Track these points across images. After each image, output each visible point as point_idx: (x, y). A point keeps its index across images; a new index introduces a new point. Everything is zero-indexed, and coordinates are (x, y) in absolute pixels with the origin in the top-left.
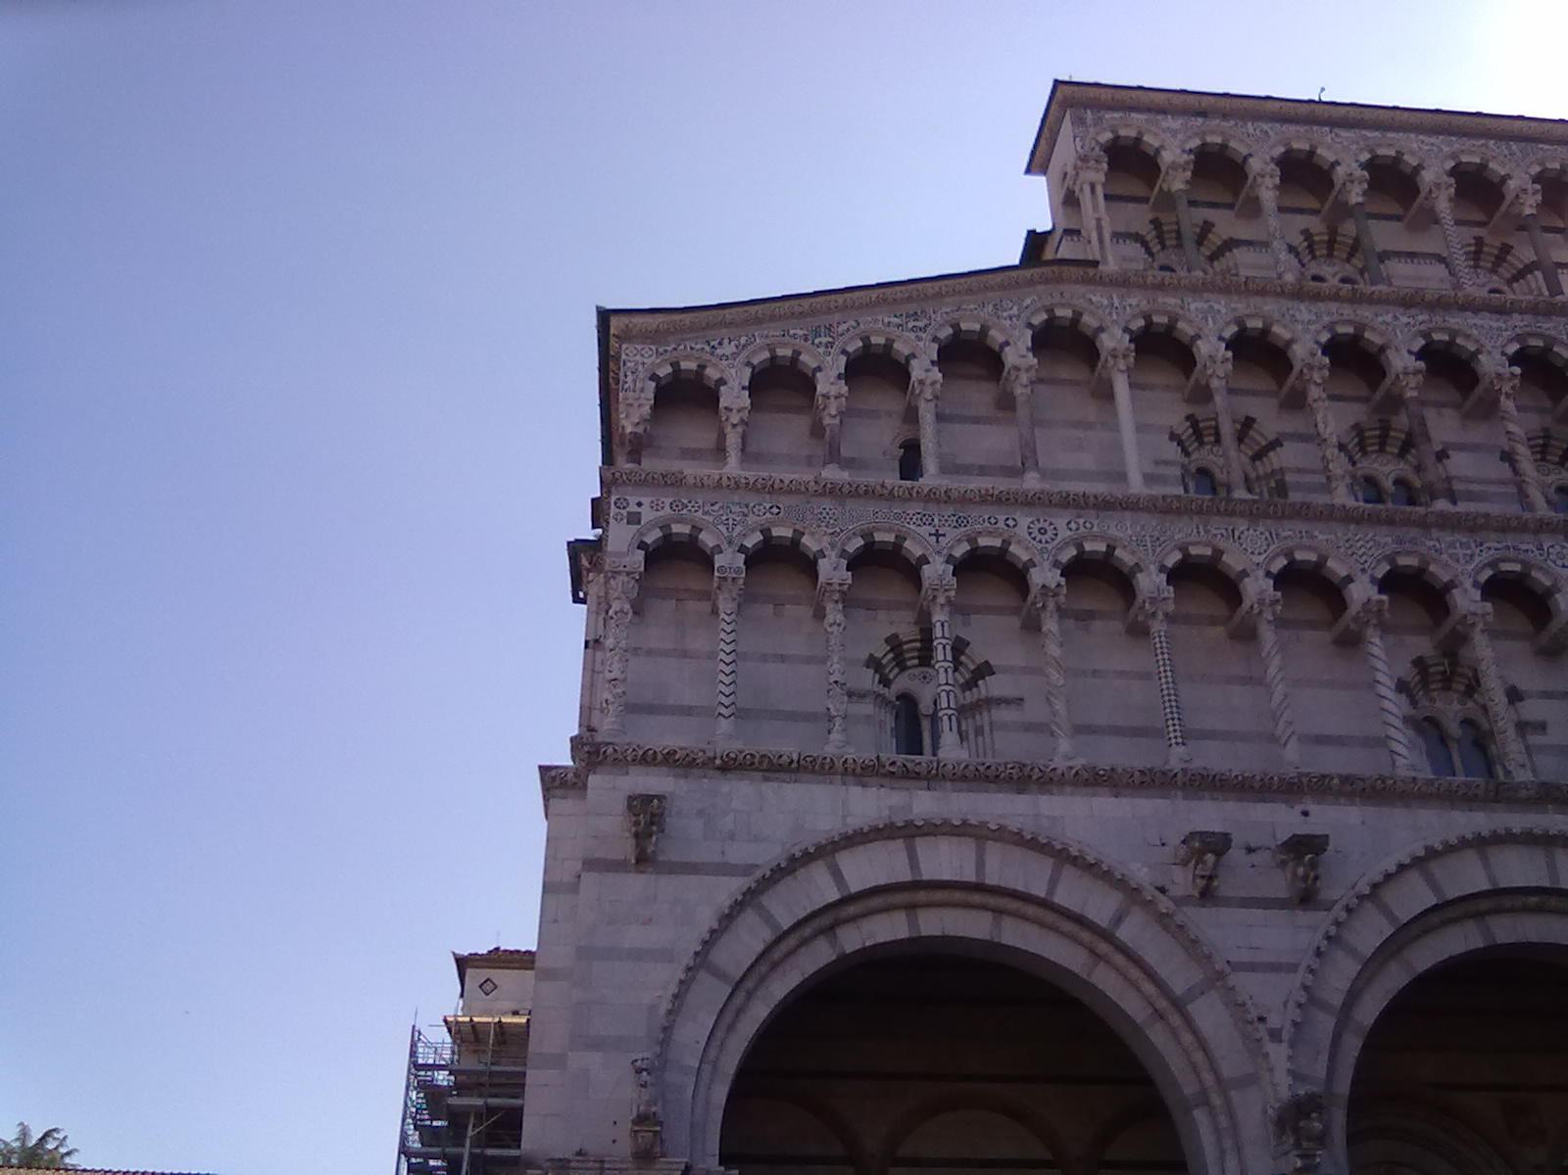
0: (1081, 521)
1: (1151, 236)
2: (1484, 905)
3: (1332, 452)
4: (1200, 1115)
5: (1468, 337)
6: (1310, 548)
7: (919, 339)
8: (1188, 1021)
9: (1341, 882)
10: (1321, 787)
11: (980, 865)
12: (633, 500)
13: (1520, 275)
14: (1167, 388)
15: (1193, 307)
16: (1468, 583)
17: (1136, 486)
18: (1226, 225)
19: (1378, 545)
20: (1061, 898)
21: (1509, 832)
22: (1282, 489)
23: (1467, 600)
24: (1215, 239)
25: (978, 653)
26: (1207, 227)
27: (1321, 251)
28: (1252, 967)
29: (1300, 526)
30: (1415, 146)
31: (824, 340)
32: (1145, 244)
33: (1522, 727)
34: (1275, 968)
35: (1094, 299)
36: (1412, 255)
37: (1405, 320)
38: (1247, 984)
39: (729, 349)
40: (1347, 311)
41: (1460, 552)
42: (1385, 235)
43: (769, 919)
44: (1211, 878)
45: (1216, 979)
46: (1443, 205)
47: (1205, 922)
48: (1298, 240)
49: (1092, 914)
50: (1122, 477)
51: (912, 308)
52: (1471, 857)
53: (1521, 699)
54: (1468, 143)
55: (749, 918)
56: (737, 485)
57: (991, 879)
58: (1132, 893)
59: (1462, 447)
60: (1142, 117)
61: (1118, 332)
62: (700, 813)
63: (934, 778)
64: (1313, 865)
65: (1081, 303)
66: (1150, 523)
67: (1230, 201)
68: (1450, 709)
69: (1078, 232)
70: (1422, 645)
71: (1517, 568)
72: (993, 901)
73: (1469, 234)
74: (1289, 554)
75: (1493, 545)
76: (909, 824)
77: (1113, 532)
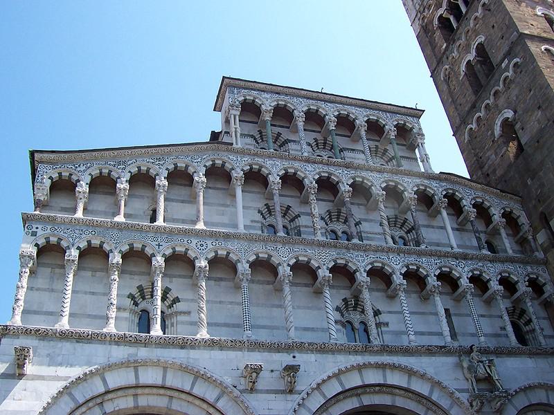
0: (217, 242)
2: (359, 391)
3: (317, 220)
5: (368, 180)
6: (305, 256)
7: (160, 168)
9: (303, 384)
10: (300, 347)
11: (164, 377)
12: (35, 226)
13: (391, 160)
14: (259, 193)
15: (268, 163)
16: (362, 270)
17: (241, 230)
18: (286, 134)
20: (196, 391)
21: (370, 363)
22: (299, 234)
23: (362, 277)
24: (282, 139)
30: (354, 111)
31: (122, 167)
32: (255, 139)
33: (378, 325)
36: (353, 150)
39: (82, 168)
40: (326, 168)
42: (341, 142)
43: (74, 399)
44: (254, 383)
46: (363, 133)
48: (312, 142)
50: (236, 226)
53: (381, 314)
54: (372, 112)
55: (66, 398)
57: (168, 384)
58: (224, 390)
59: (365, 220)
61: (239, 170)
62: (48, 355)
63: (147, 343)
68: (356, 318)
69: (228, 133)
70: (346, 294)
71: (380, 265)
72: (169, 393)
73: (373, 144)
74: (297, 258)
75: (372, 257)
76: (136, 361)
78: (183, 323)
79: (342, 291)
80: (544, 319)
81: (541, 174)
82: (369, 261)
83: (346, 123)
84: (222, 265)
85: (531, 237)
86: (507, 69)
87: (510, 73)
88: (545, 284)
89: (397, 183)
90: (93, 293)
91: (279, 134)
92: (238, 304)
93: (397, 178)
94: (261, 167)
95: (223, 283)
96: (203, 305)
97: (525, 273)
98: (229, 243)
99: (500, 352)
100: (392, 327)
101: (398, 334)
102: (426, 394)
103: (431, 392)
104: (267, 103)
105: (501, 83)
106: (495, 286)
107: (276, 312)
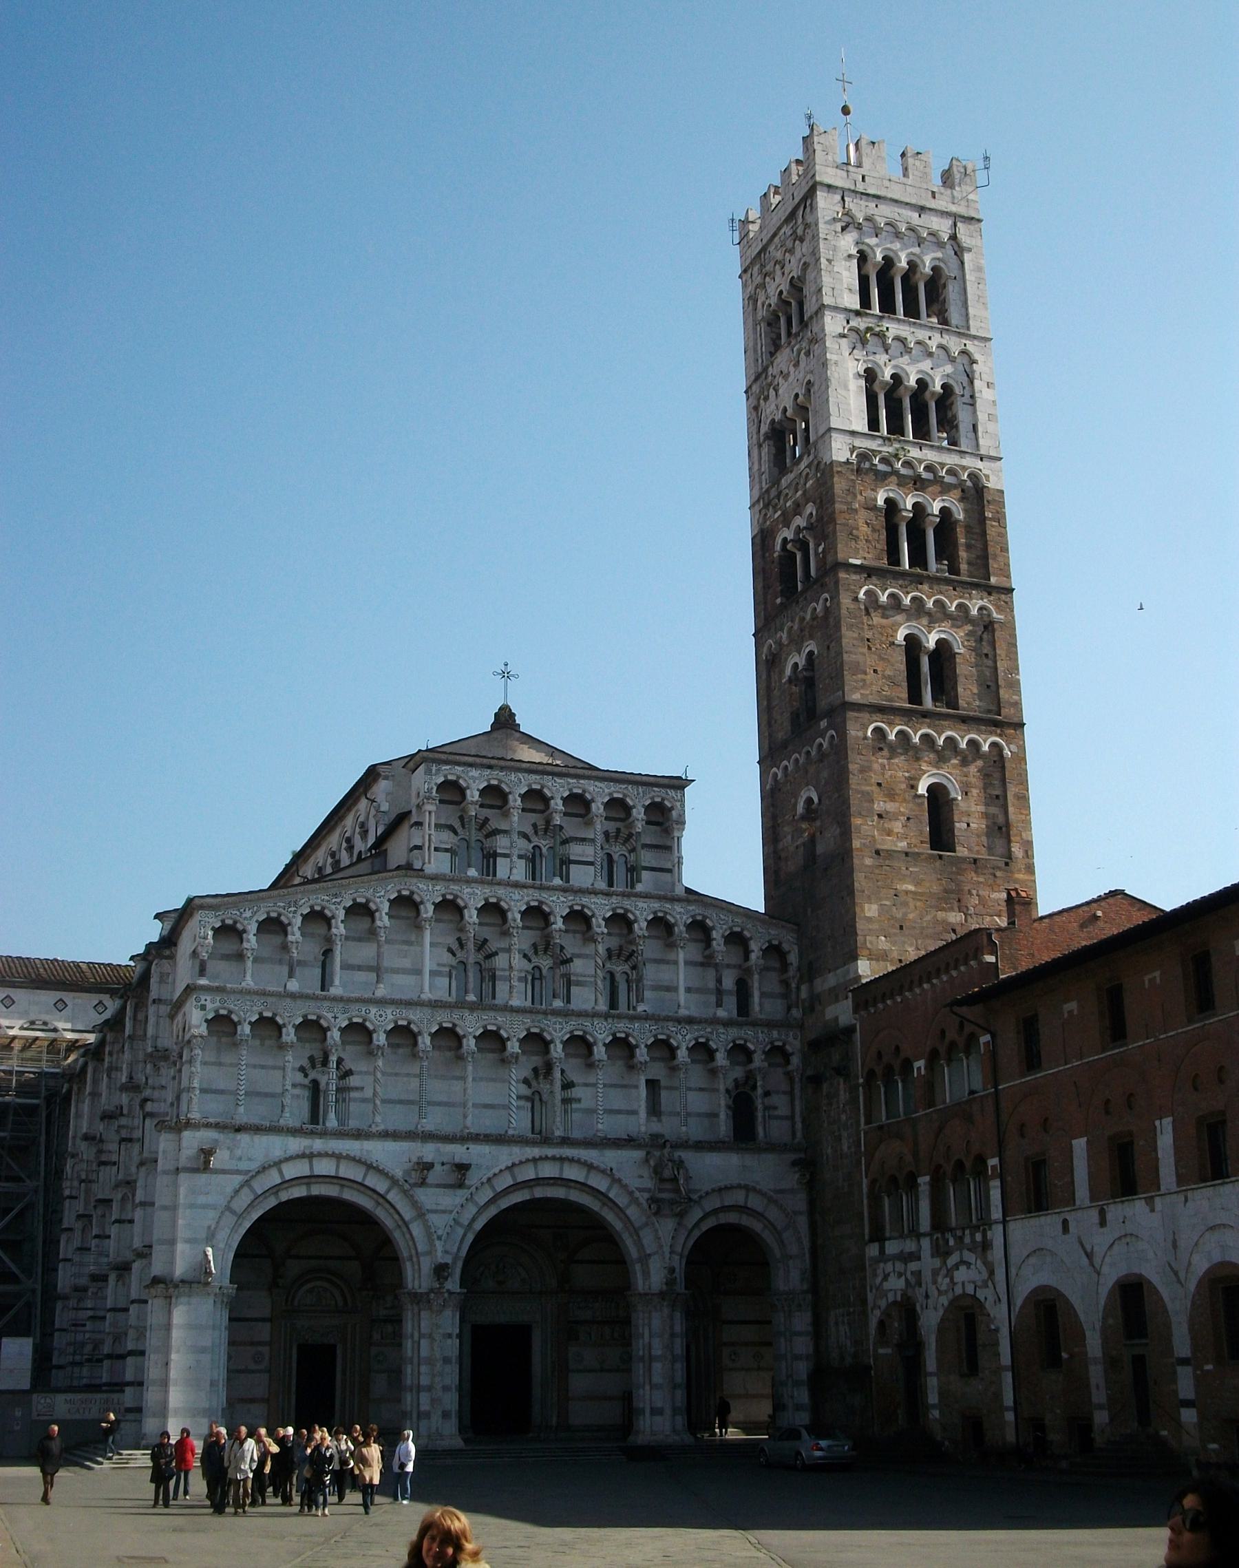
1: (457, 825)
2: (532, 1183)
4: (408, 1264)
5: (589, 908)
7: (337, 909)
8: (408, 1229)
9: (473, 1178)
10: (476, 1138)
12: (203, 998)
13: (633, 850)
19: (524, 1023)
20: (366, 1183)
23: (557, 1050)
25: (348, 1065)
26: (486, 820)
28: (435, 1212)
29: (492, 1014)
30: (592, 789)
33: (565, 1101)
34: (444, 1212)
35: (421, 886)
36: (583, 840)
37: (562, 899)
38: (432, 1218)
39: (248, 914)
40: (536, 894)
41: (558, 1026)
42: (572, 828)
45: (421, 1214)
47: (423, 1195)
48: (529, 830)
49: (378, 1189)
51: (334, 891)
52: (531, 1165)
55: (246, 1190)
56: (249, 992)
58: (394, 1182)
59: (579, 956)
63: (324, 1134)
64: (464, 1175)
65: (414, 888)
66: (427, 1011)
67: (499, 804)
68: (544, 1087)
70: (536, 1060)
73: (612, 826)
77: (412, 1017)
78: (355, 1100)
79: (535, 1058)
80: (784, 1093)
82: (569, 1028)
83: (578, 804)
84: (404, 1034)
85: (793, 985)
88: (792, 1054)
89: (627, 911)
90: (263, 1067)
91: (486, 820)
92: (415, 1076)
93: (627, 903)
94: (456, 896)
95: (401, 1051)
98: (411, 1012)
99: (700, 1146)
100: (582, 1105)
101: (591, 1111)
102: (603, 1189)
103: (609, 1189)
104: (475, 782)
105: (815, 746)
106: (721, 1059)
107: (457, 1086)
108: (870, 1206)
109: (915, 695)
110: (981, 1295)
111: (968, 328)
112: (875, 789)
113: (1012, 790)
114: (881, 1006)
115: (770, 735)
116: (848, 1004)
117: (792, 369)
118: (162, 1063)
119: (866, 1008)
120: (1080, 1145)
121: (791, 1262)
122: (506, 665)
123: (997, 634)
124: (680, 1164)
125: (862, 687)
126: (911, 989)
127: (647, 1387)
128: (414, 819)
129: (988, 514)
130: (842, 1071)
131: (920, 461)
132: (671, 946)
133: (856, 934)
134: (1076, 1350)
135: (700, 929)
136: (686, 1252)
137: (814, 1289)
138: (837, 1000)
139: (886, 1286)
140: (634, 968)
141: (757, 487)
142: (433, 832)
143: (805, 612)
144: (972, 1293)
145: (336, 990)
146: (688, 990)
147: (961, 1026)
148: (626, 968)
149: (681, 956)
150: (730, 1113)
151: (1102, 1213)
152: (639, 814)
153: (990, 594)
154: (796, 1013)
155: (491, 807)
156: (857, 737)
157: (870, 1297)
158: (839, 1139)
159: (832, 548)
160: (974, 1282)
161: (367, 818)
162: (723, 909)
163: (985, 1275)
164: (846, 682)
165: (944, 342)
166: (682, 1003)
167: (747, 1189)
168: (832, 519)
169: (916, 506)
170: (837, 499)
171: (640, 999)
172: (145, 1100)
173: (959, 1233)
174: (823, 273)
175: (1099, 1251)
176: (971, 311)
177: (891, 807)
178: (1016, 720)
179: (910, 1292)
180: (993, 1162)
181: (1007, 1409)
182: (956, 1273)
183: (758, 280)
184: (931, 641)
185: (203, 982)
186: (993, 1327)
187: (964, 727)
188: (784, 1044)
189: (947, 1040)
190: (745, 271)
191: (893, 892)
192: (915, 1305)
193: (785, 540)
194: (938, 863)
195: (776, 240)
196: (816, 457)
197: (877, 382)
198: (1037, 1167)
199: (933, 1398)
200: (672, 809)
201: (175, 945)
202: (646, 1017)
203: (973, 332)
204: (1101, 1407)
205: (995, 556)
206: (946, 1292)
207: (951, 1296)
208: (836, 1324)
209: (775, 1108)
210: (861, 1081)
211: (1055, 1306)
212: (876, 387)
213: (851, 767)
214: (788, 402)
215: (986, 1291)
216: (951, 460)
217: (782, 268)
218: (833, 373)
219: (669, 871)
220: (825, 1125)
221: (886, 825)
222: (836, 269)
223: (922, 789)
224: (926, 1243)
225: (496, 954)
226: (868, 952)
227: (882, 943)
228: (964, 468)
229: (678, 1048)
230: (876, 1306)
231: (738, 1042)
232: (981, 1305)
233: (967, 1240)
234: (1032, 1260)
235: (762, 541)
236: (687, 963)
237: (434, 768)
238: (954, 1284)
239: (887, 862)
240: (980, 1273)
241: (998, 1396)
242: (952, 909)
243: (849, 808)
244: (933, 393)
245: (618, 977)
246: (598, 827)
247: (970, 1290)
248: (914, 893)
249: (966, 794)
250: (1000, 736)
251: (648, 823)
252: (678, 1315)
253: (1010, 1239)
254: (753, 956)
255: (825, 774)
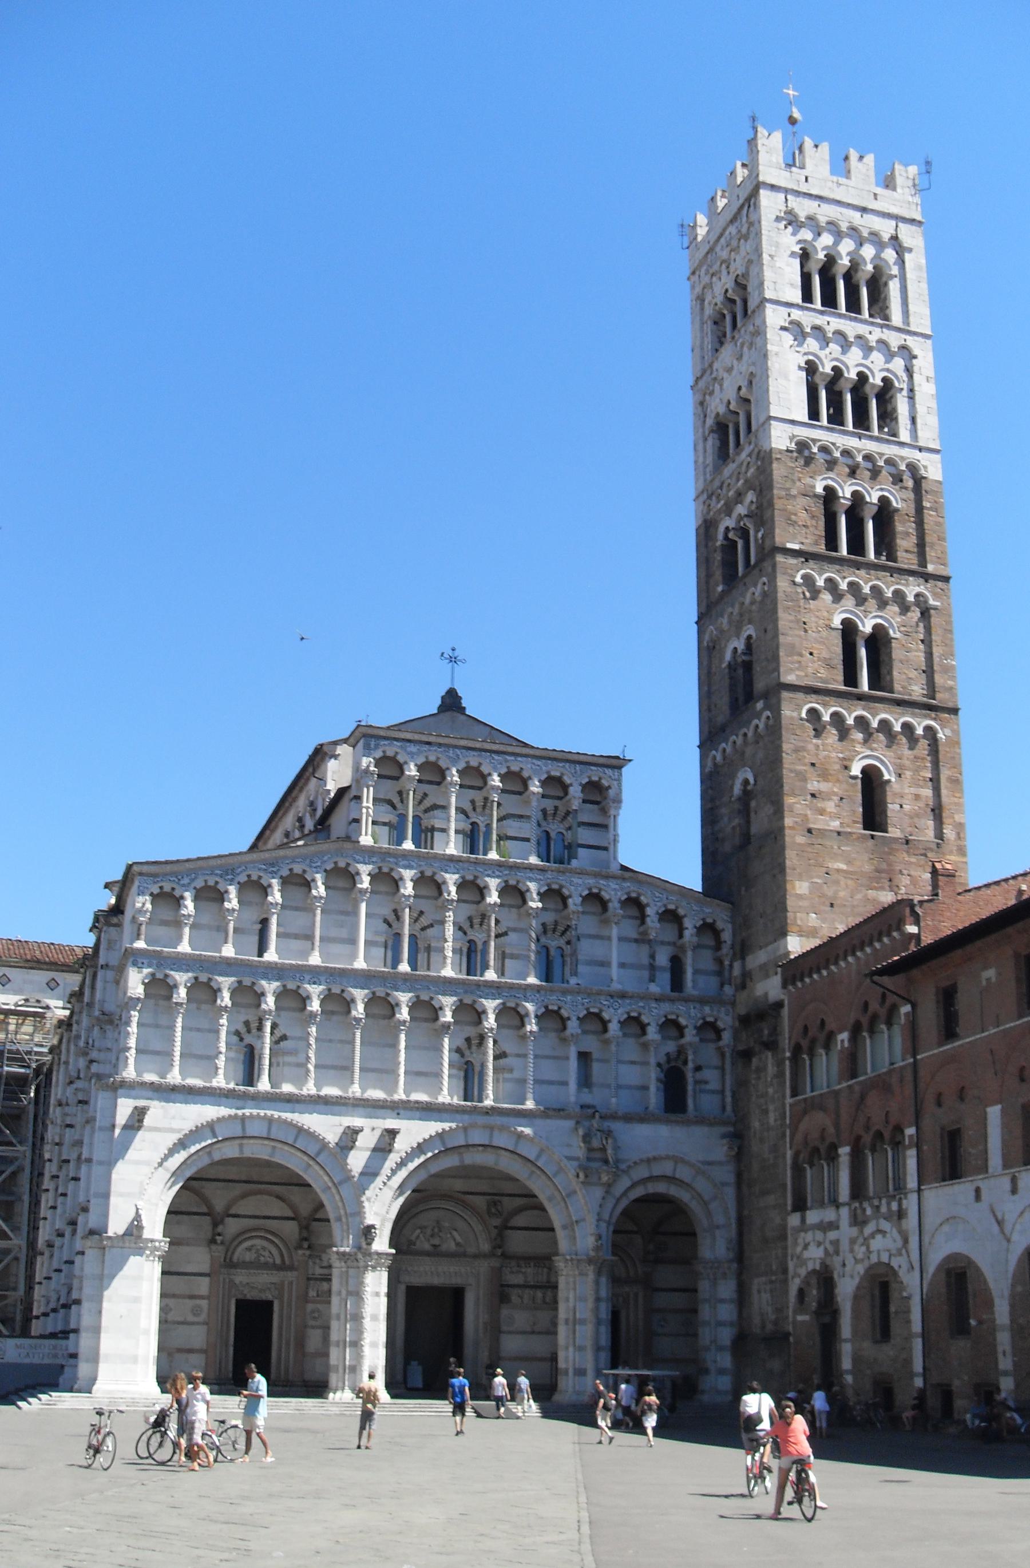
1: (396, 800)
13: (570, 828)
14: (387, 893)
27: (479, 810)
36: (521, 817)
39: (186, 881)
48: (468, 807)
59: (514, 930)
60: (398, 744)
72: (272, 1144)
80: (716, 1068)
81: (753, 890)
86: (758, 715)
87: (761, 726)
88: (724, 1029)
89: (561, 887)
90: (198, 1030)
93: (562, 879)
95: (335, 1018)
96: (312, 1041)
97: (699, 1015)
99: (628, 1118)
106: (652, 1033)
108: (793, 1178)
109: (851, 678)
110: (894, 1263)
111: (908, 324)
112: (808, 768)
113: (945, 773)
114: (807, 980)
115: (710, 720)
116: (776, 980)
117: (735, 362)
118: (108, 1027)
119: (794, 984)
120: (994, 1113)
121: (717, 1232)
122: (453, 650)
123: (933, 620)
124: (608, 1134)
125: (798, 669)
126: (836, 963)
127: (571, 1349)
128: (353, 792)
129: (926, 504)
130: (771, 1045)
131: (859, 451)
132: (606, 922)
133: (786, 911)
134: (984, 1317)
135: (634, 905)
136: (614, 1220)
137: (740, 1256)
138: (767, 976)
139: (806, 1255)
140: (568, 943)
141: (702, 478)
142: (370, 805)
143: (744, 597)
144: (887, 1261)
145: (271, 956)
146: (622, 965)
147: (884, 996)
148: (562, 942)
149: (615, 932)
150: (662, 1086)
151: (1014, 1180)
152: (575, 791)
153: (926, 581)
154: (728, 990)
155: (430, 782)
156: (792, 718)
157: (791, 1265)
158: (766, 1112)
159: (770, 533)
160: (888, 1251)
161: (316, 797)
162: (658, 887)
163: (900, 1243)
164: (782, 663)
165: (884, 337)
166: (615, 978)
167: (677, 1160)
168: (771, 505)
169: (855, 494)
170: (775, 484)
171: (575, 973)
172: (92, 1061)
173: (876, 1202)
174: (765, 268)
175: (1010, 1218)
176: (911, 307)
177: (824, 787)
178: (950, 705)
179: (828, 1262)
180: (910, 1131)
181: (917, 1375)
182: (872, 1242)
183: (706, 279)
184: (866, 627)
185: (141, 944)
186: (905, 1294)
187: (899, 710)
188: (716, 1020)
189: (870, 1013)
190: (693, 273)
191: (824, 870)
192: (832, 1272)
193: (727, 528)
194: (871, 842)
195: (723, 240)
196: (756, 445)
197: (818, 374)
198: (953, 1138)
199: (846, 1364)
200: (609, 787)
201: (122, 912)
202: (578, 991)
203: (913, 328)
204: (1006, 1373)
205: (933, 545)
206: (862, 1260)
207: (866, 1264)
208: (759, 1292)
209: (706, 1082)
210: (788, 1054)
211: (965, 1272)
212: (817, 379)
213: (786, 747)
214: (730, 394)
215: (899, 1258)
216: (890, 450)
217: (728, 267)
218: (773, 364)
219: (606, 849)
220: (754, 1099)
221: (819, 805)
222: (778, 264)
223: (856, 770)
224: (844, 1212)
225: (432, 926)
226: (798, 928)
227: (813, 919)
228: (902, 458)
229: (609, 1021)
230: (796, 1275)
231: (669, 1017)
232: (895, 1273)
233: (884, 1209)
234: (946, 1228)
235: (706, 529)
236: (621, 939)
237: (373, 743)
238: (870, 1252)
239: (820, 841)
240: (895, 1241)
241: (908, 1362)
242: (882, 888)
243: (782, 786)
244: (874, 385)
245: (552, 952)
246: (534, 804)
247: (885, 1259)
248: (843, 871)
249: (900, 775)
250: (935, 719)
251: (584, 801)
252: (603, 1280)
253: (924, 1209)
254: (687, 933)
255: (761, 755)
